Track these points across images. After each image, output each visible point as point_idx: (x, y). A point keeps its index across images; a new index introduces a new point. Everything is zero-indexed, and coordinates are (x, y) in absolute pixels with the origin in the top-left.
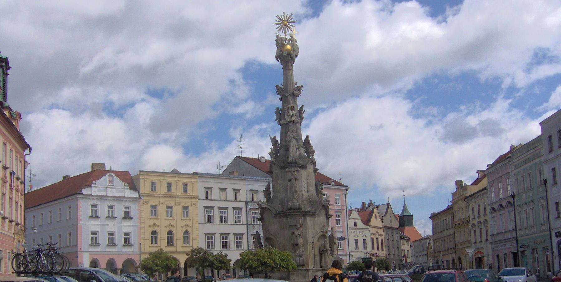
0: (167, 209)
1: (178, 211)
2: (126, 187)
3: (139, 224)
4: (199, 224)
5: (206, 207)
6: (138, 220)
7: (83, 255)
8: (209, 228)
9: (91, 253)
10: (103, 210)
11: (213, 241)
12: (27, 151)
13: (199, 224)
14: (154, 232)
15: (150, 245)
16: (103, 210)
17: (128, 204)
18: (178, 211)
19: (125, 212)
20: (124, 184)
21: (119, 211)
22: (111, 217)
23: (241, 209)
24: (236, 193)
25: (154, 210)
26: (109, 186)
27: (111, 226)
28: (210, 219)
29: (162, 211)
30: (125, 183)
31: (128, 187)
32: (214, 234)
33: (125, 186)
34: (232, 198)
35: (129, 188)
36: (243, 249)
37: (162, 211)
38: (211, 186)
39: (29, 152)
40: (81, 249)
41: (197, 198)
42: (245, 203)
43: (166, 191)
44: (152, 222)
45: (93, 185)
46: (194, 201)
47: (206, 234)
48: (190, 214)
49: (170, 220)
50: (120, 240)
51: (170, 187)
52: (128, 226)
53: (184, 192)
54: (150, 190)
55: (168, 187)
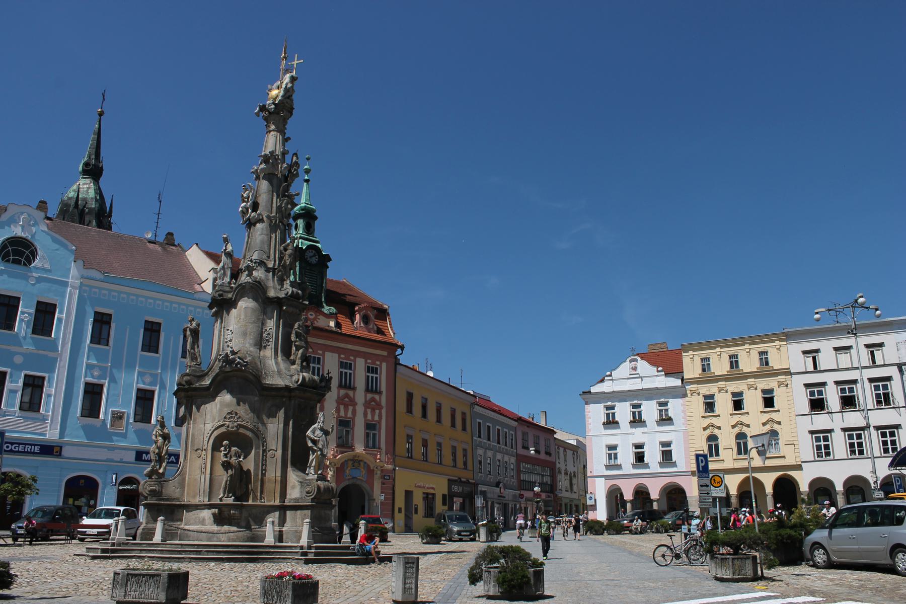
1: (753, 401)
3: (686, 427)
4: (797, 415)
5: (807, 386)
7: (595, 481)
8: (821, 421)
9: (607, 477)
10: (623, 412)
12: (399, 351)
13: (797, 415)
15: (735, 458)
16: (623, 412)
18: (753, 401)
20: (656, 368)
23: (889, 379)
24: (872, 353)
27: (638, 435)
28: (817, 405)
29: (724, 403)
30: (657, 369)
31: (663, 373)
32: (830, 431)
34: (866, 361)
36: (834, 457)
37: (724, 403)
39: (401, 352)
40: (591, 472)
41: (788, 373)
42: (896, 367)
45: (606, 378)
46: (781, 378)
47: (812, 432)
49: (739, 416)
50: (653, 456)
51: (737, 362)
52: (666, 434)
53: (762, 364)
54: (700, 372)
55: (731, 362)
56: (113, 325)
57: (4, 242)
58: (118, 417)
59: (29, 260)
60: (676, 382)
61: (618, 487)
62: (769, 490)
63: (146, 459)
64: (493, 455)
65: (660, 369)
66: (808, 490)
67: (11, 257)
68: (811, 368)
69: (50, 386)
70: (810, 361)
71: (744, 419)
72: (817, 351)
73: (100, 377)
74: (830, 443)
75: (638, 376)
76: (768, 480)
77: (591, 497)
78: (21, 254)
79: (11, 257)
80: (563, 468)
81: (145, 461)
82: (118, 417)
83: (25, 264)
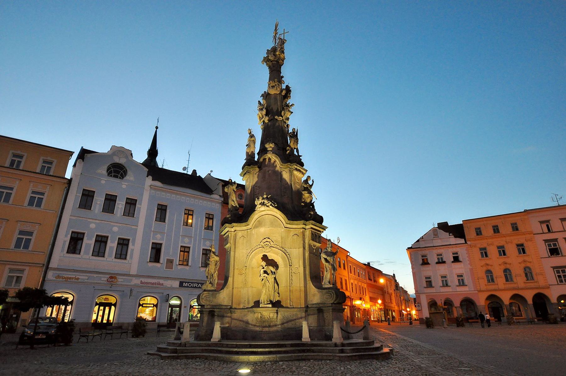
0: (498, 249)
1: (511, 250)
2: (450, 236)
4: (541, 258)
5: (546, 241)
6: (468, 262)
11: (557, 275)
14: (489, 272)
17: (440, 251)
18: (511, 250)
19: (454, 257)
21: (449, 258)
22: (441, 262)
25: (484, 253)
26: (434, 238)
27: (442, 270)
29: (493, 251)
30: (449, 234)
31: (453, 236)
33: (450, 235)
35: (454, 236)
37: (493, 251)
38: (549, 219)
41: (531, 233)
43: (493, 233)
44: (483, 263)
46: (528, 236)
47: (554, 268)
48: (527, 250)
50: (453, 281)
52: (458, 268)
54: (476, 235)
56: (168, 211)
57: (109, 166)
58: (170, 262)
59: (122, 177)
60: (462, 241)
61: (433, 300)
62: (530, 301)
63: (185, 286)
64: (357, 283)
65: (450, 234)
66: (532, 303)
67: (113, 174)
68: (546, 230)
69: (133, 245)
70: (544, 226)
71: (508, 261)
72: (548, 221)
73: (160, 240)
74: (557, 275)
75: (438, 238)
76: (529, 296)
77: (419, 306)
78: (118, 172)
79: (113, 174)
80: (387, 291)
81: (184, 287)
82: (170, 262)
83: (120, 178)
